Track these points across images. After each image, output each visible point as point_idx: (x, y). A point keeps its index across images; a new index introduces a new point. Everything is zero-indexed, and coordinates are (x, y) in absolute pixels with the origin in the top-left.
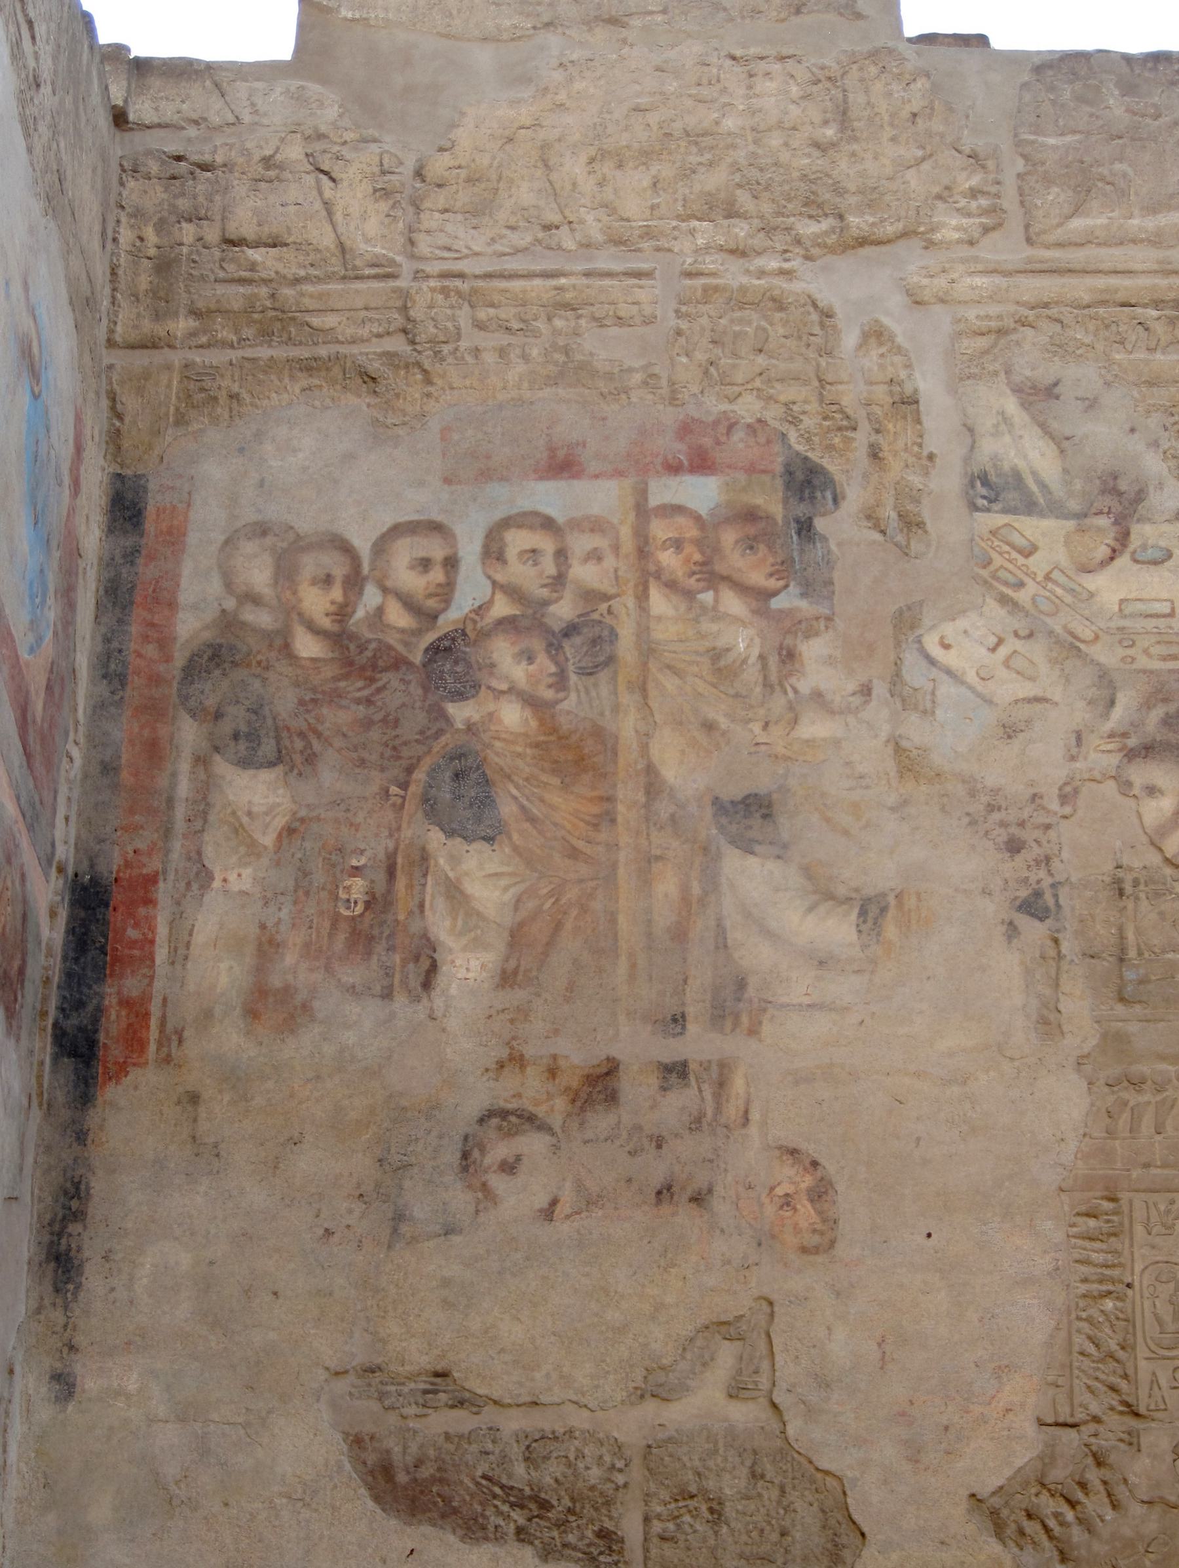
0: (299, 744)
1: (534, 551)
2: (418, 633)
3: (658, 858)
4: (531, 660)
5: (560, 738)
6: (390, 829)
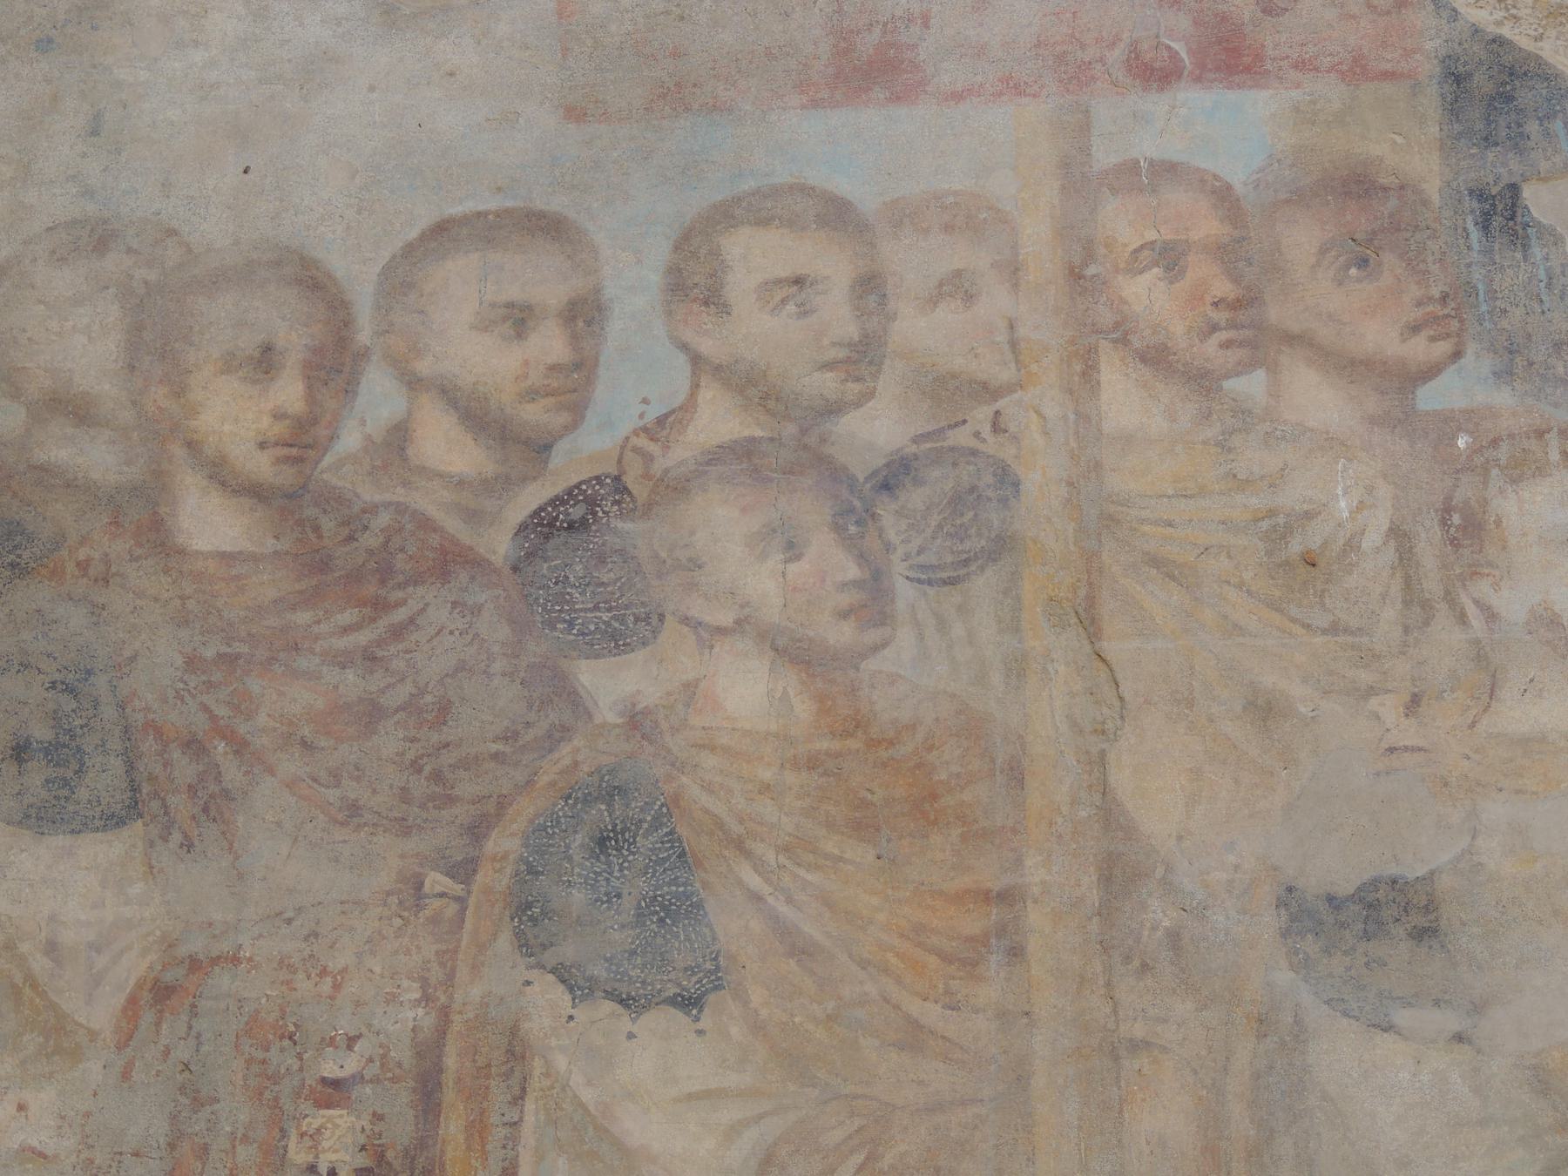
0: (185, 769)
1: (798, 281)
2: (499, 486)
3: (1135, 1046)
4: (793, 550)
5: (873, 744)
6: (424, 983)
